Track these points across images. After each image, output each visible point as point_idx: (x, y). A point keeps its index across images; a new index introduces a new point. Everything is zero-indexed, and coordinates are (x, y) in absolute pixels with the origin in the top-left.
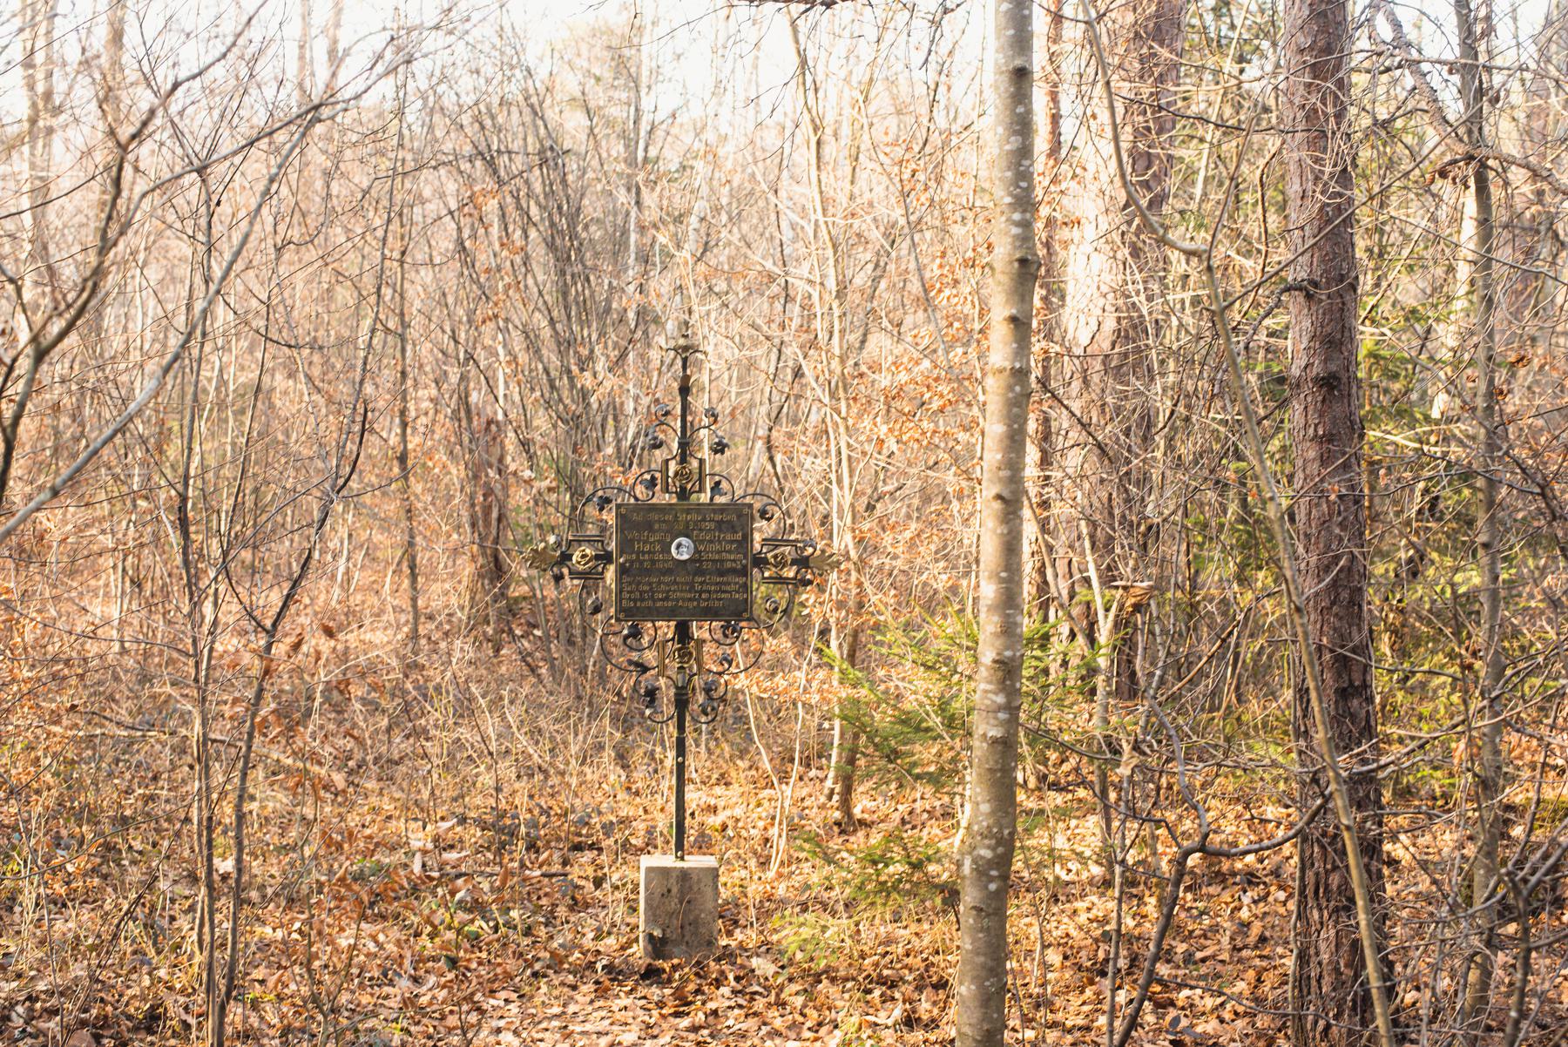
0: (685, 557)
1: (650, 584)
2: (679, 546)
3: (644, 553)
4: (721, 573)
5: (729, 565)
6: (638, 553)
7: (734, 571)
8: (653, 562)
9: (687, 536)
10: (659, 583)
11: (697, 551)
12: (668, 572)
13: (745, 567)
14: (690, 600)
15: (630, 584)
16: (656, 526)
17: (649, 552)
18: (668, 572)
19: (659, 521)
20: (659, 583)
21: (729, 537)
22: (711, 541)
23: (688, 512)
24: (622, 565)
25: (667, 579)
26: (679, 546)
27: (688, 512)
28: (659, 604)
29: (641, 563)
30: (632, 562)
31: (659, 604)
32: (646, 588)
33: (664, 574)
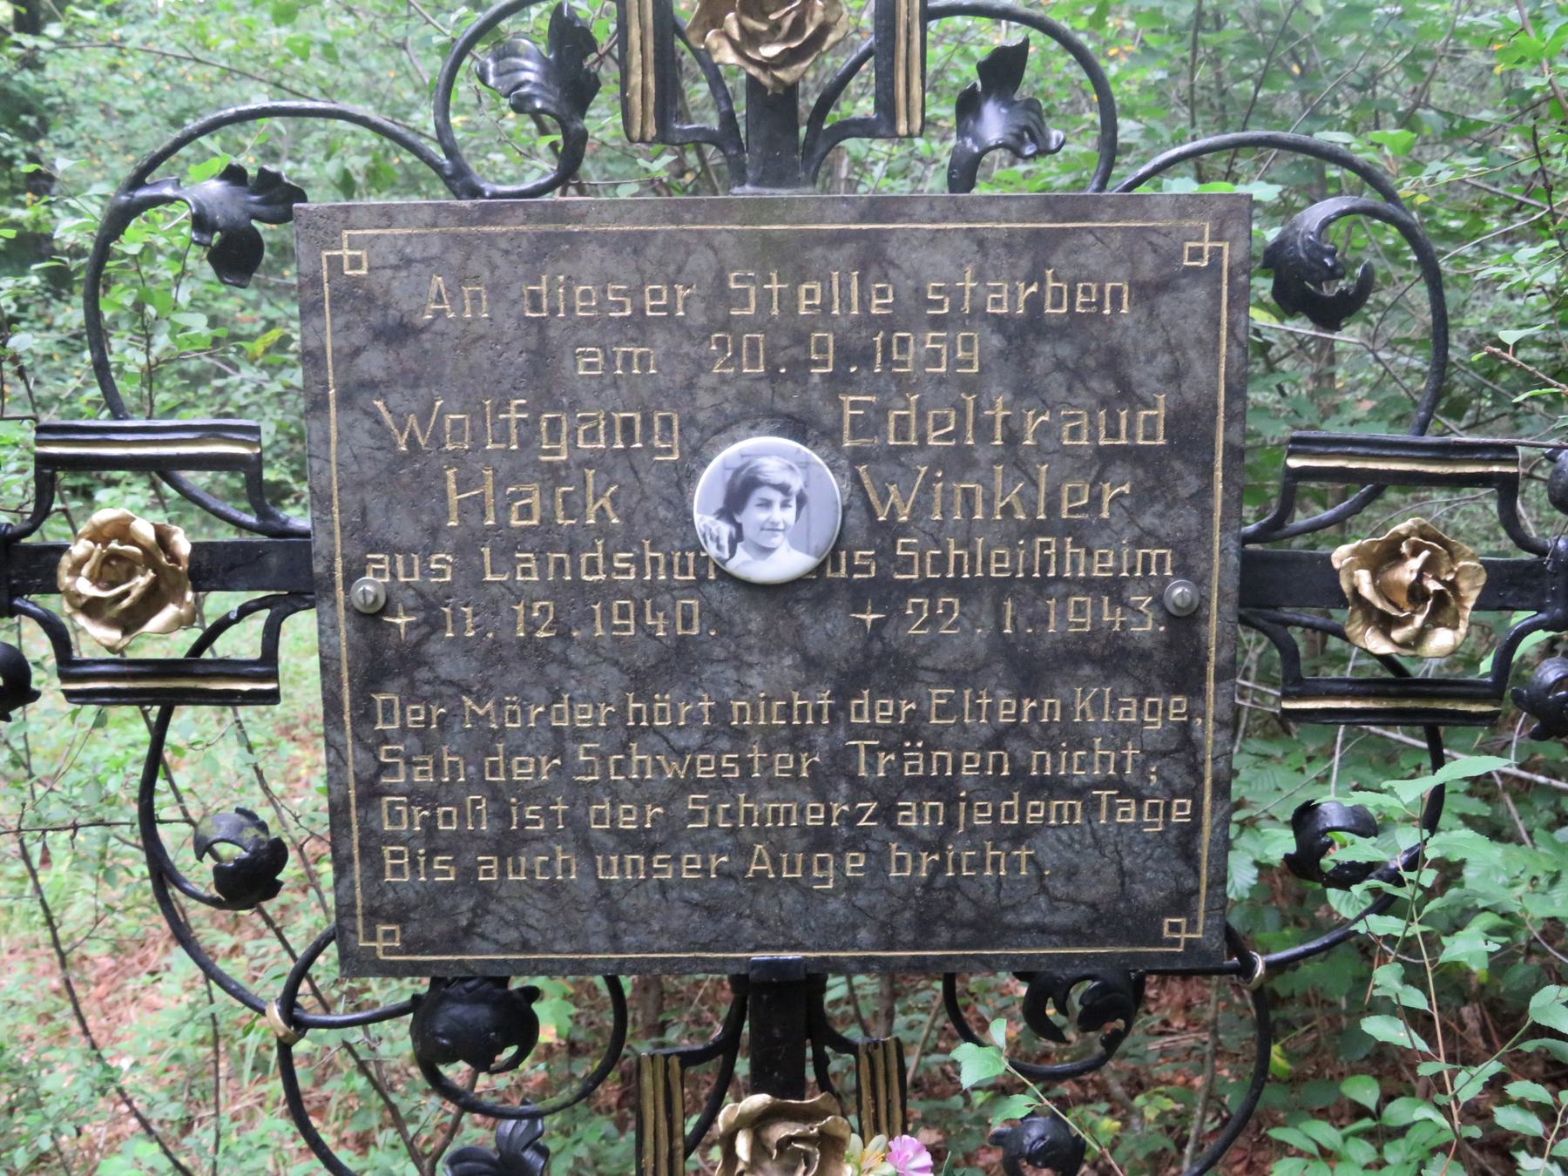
0: (787, 562)
1: (559, 741)
2: (740, 492)
3: (508, 545)
4: (1029, 670)
5: (1070, 618)
6: (466, 548)
7: (1111, 657)
8: (574, 598)
9: (797, 427)
10: (625, 735)
11: (865, 525)
12: (677, 662)
13: (1184, 623)
14: (821, 839)
15: (427, 741)
16: (585, 365)
17: (545, 538)
18: (677, 662)
19: (608, 330)
20: (625, 735)
21: (1083, 429)
22: (959, 461)
23: (790, 257)
24: (371, 618)
25: (670, 707)
30: (430, 608)
33: (642, 682)
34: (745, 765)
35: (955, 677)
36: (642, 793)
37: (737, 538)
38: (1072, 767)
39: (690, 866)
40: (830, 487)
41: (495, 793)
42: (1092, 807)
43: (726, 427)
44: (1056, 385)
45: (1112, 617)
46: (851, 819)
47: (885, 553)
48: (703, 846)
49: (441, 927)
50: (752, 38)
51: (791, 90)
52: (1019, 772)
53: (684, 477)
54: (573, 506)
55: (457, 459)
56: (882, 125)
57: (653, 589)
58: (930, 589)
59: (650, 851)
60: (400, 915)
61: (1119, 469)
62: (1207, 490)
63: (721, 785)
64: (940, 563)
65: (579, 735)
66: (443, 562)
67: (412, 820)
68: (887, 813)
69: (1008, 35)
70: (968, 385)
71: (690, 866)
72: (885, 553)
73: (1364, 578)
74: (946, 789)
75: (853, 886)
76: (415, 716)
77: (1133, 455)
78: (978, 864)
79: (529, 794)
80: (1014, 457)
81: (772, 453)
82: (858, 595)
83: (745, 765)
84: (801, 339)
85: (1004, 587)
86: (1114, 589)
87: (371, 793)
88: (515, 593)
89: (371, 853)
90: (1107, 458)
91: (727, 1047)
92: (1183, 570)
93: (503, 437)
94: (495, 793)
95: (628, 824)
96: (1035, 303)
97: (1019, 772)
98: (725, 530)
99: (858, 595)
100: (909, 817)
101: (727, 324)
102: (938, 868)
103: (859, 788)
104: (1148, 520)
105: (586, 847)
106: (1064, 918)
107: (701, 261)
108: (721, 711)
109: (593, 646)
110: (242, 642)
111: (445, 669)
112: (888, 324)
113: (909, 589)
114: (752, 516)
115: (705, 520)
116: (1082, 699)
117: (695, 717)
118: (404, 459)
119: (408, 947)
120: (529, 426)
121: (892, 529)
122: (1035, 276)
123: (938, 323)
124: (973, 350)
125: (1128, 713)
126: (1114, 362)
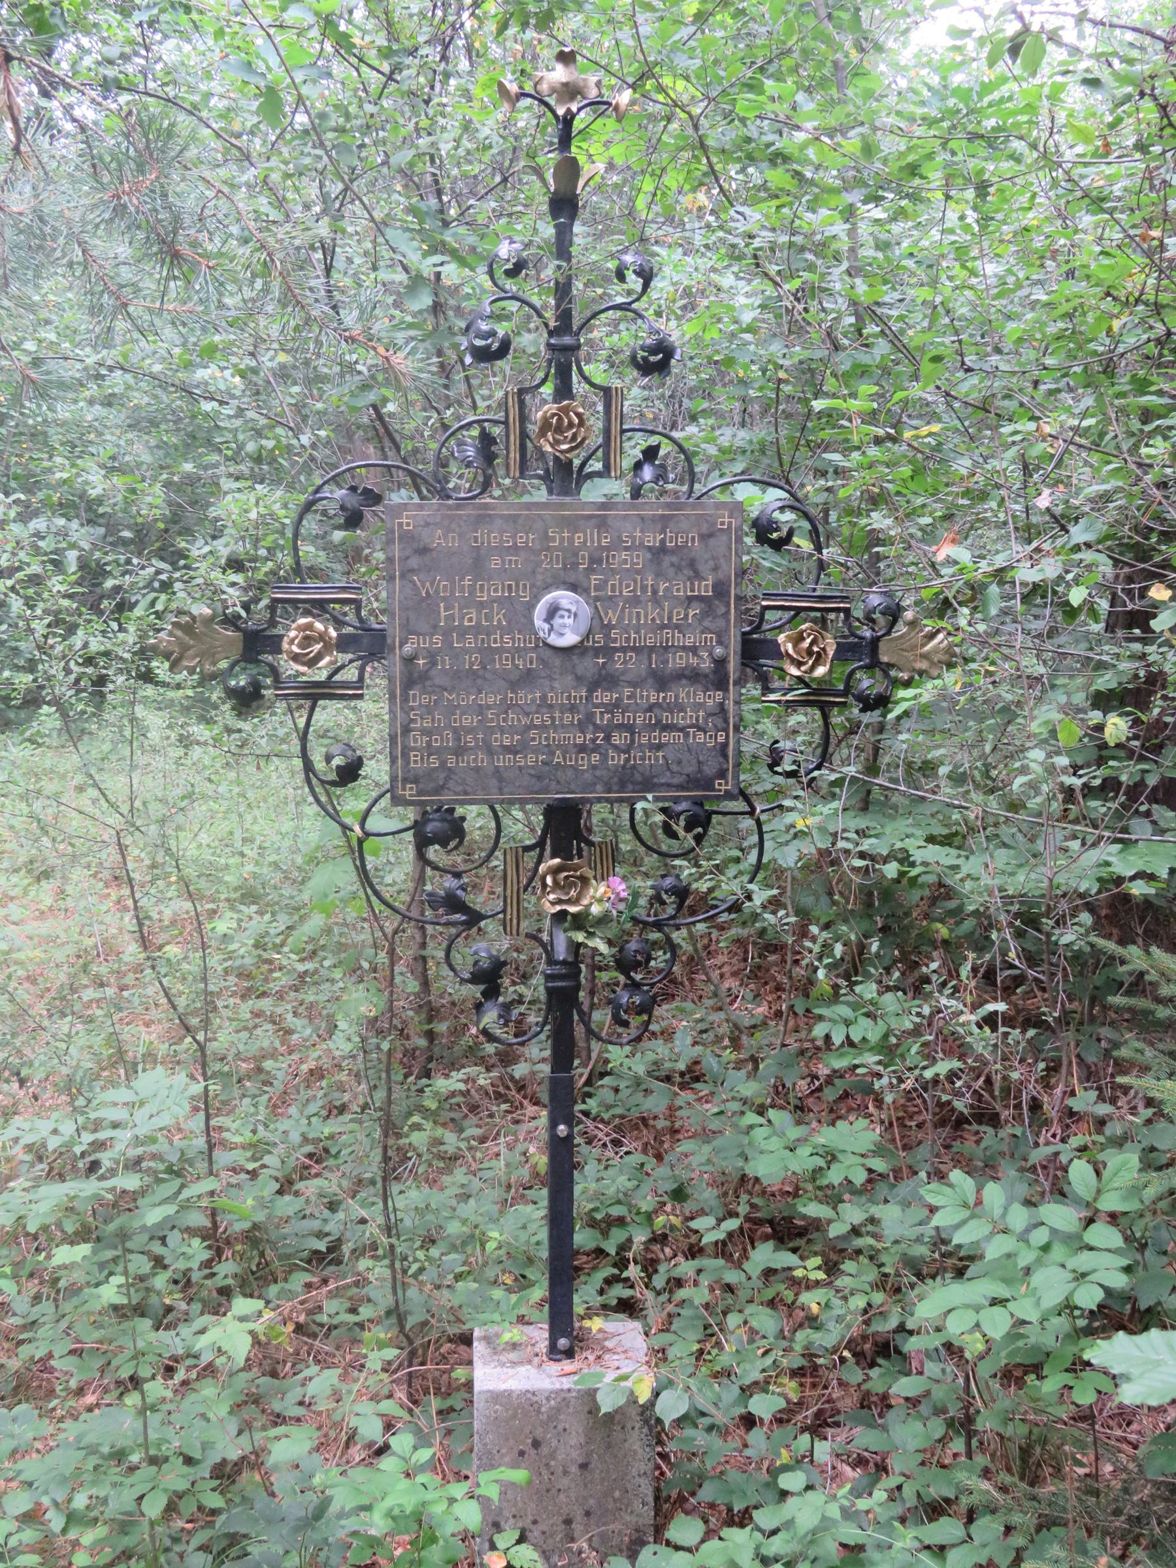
0: (570, 639)
1: (481, 710)
2: (553, 612)
3: (463, 632)
4: (662, 681)
5: (678, 661)
6: (447, 634)
7: (693, 676)
8: (488, 653)
9: (574, 588)
11: (599, 625)
12: (527, 678)
13: (721, 663)
14: (582, 749)
15: (429, 710)
16: (495, 563)
17: (477, 630)
18: (527, 678)
19: (502, 551)
21: (681, 590)
22: (635, 601)
23: (572, 524)
24: (409, 660)
25: (526, 697)
26: (553, 612)
27: (572, 524)
28: (503, 761)
29: (456, 655)
30: (432, 657)
31: (503, 761)
32: (469, 721)
33: (514, 686)
34: (553, 719)
35: (634, 684)
36: (512, 730)
37: (551, 629)
38: (679, 719)
39: (531, 759)
40: (586, 610)
41: (455, 731)
42: (687, 735)
43: (547, 588)
44: (671, 572)
45: (694, 661)
46: (594, 740)
47: (607, 636)
48: (536, 751)
49: (432, 785)
50: (557, 442)
51: (571, 462)
52: (659, 722)
53: (531, 607)
54: (489, 618)
55: (444, 599)
56: (605, 473)
57: (518, 650)
58: (624, 650)
59: (515, 753)
60: (416, 781)
61: (695, 604)
62: (728, 612)
63: (543, 727)
64: (628, 639)
65: (489, 707)
66: (438, 638)
67: (422, 741)
68: (607, 738)
69: (654, 440)
70: (638, 572)
71: (531, 759)
72: (607, 636)
73: (790, 646)
74: (630, 728)
75: (594, 767)
76: (425, 699)
77: (699, 598)
78: (643, 758)
79: (470, 730)
80: (656, 600)
81: (564, 597)
82: (597, 652)
83: (553, 719)
84: (576, 555)
85: (652, 649)
86: (694, 650)
87: (406, 730)
88: (465, 651)
89: (405, 755)
90: (690, 599)
91: (541, 844)
92: (720, 643)
93: (462, 590)
94: (455, 731)
95: (507, 743)
96: (663, 541)
97: (659, 722)
98: (546, 626)
99: (597, 652)
100: (616, 740)
101: (548, 549)
102: (627, 760)
103: (597, 728)
104: (706, 623)
105: (490, 752)
106: (676, 780)
107: (539, 525)
108: (544, 697)
109: (495, 672)
110: (351, 674)
111: (437, 681)
112: (608, 549)
113: (616, 650)
114: (557, 621)
115: (539, 622)
116: (684, 693)
117: (533, 700)
118: (423, 599)
119: (419, 793)
120: (472, 588)
121: (610, 627)
122: (663, 531)
123: (626, 549)
124: (640, 559)
125: (700, 698)
126: (692, 564)
